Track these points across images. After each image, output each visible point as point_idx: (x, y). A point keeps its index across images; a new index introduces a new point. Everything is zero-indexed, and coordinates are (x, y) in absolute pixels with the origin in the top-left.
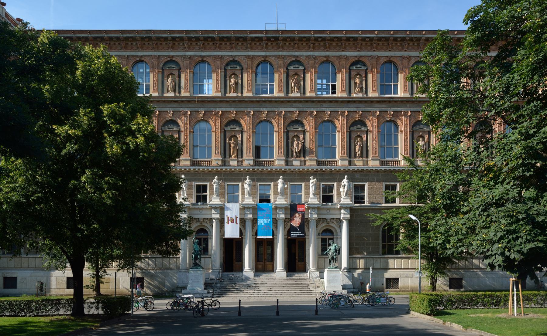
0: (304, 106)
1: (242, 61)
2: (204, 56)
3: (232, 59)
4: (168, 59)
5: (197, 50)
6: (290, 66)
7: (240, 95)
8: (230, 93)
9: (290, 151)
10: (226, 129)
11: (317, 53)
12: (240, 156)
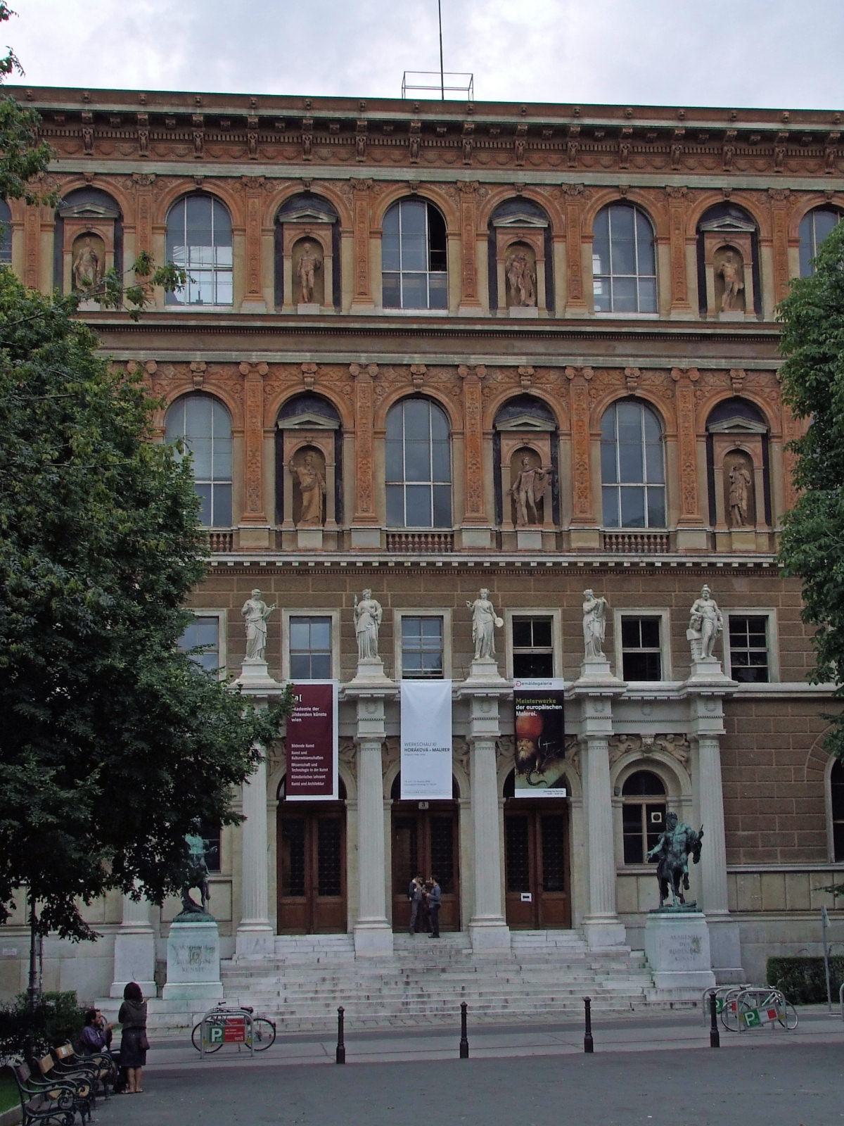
0: (551, 351)
1: (336, 193)
2: (206, 177)
3: (300, 189)
4: (78, 185)
5: (181, 158)
6: (499, 216)
7: (330, 311)
10: (285, 424)
11: (589, 178)
12: (331, 519)
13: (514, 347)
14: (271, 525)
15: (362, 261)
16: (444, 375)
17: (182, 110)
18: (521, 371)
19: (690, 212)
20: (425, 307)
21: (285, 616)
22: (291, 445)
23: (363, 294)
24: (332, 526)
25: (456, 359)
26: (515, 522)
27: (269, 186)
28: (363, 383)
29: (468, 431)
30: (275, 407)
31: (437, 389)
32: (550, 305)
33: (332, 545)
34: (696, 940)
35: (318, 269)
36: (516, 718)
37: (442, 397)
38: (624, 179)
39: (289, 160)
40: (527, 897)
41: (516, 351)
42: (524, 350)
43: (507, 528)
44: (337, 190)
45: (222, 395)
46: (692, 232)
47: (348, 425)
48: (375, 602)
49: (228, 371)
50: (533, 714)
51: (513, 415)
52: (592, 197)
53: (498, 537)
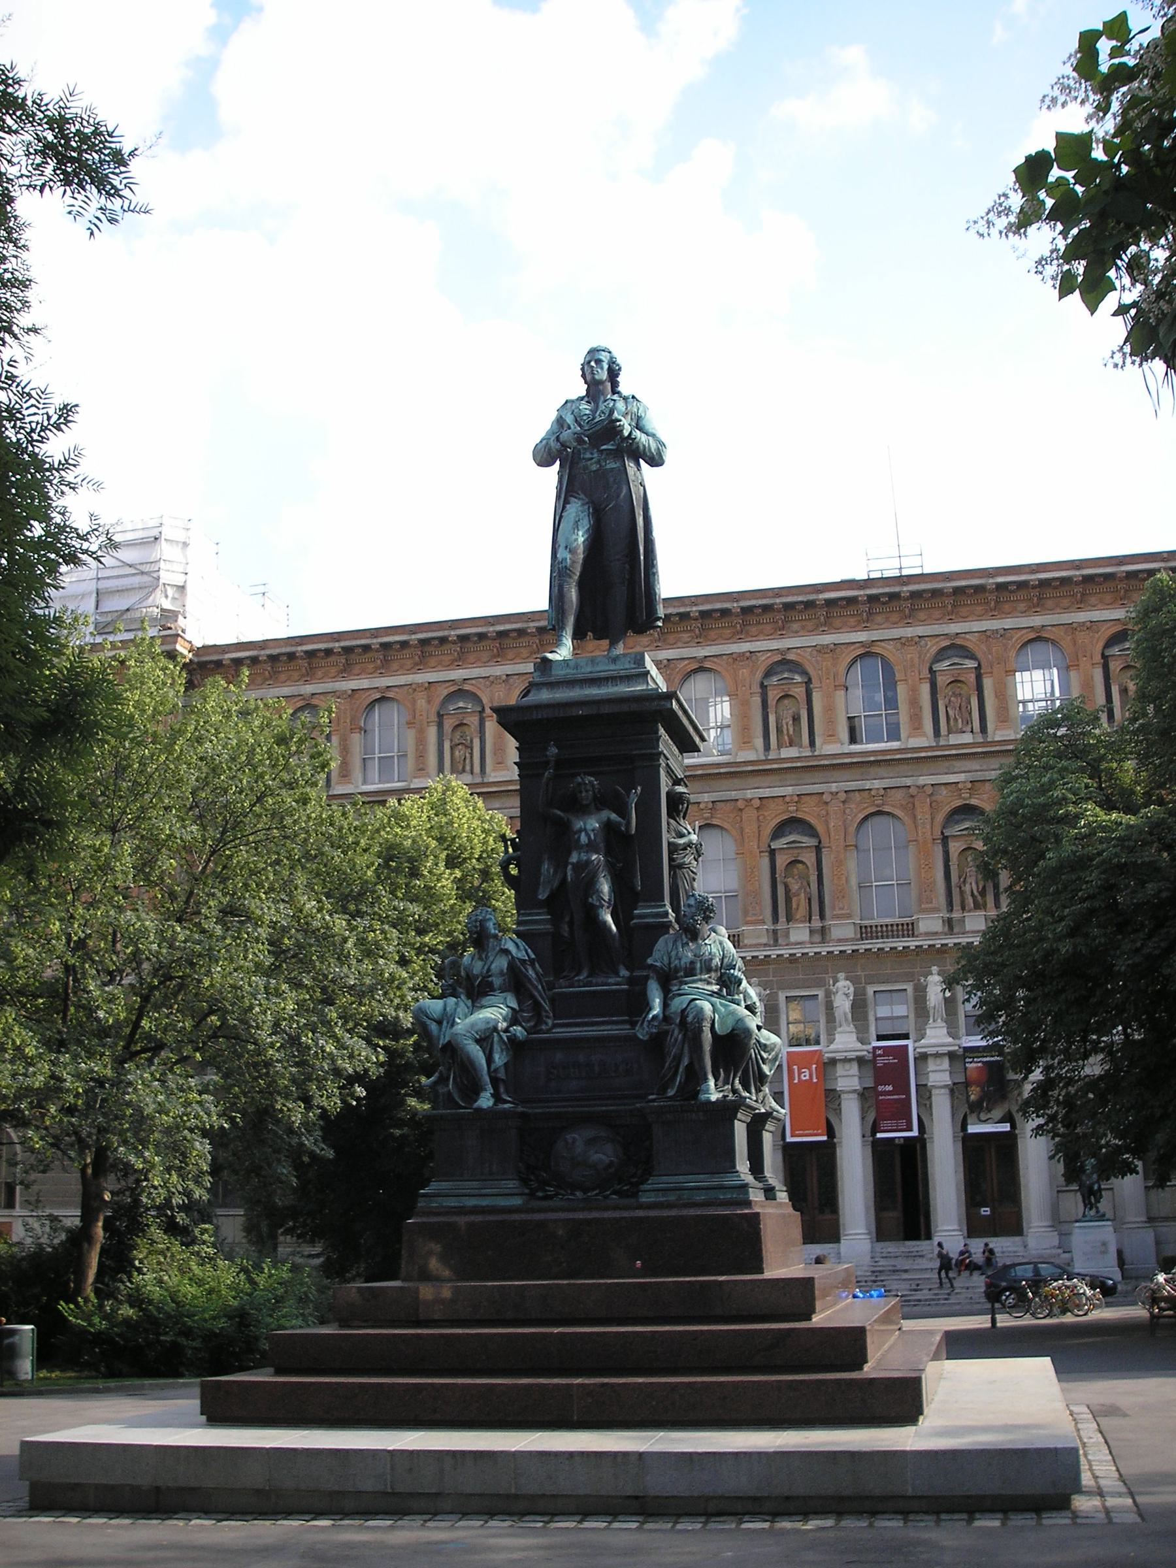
0: (985, 767)
3: (778, 658)
5: (686, 644)
6: (938, 661)
8: (779, 747)
9: (955, 892)
11: (1008, 623)
12: (816, 917)
13: (954, 767)
14: (769, 926)
15: (830, 709)
16: (899, 795)
17: (682, 610)
18: (960, 786)
19: (1095, 641)
20: (881, 740)
21: (782, 996)
22: (782, 861)
23: (831, 736)
24: (816, 923)
25: (908, 782)
26: (963, 909)
27: (754, 658)
28: (835, 807)
29: (920, 839)
30: (768, 831)
31: (893, 806)
32: (984, 729)
33: (817, 938)
34: (1104, 1244)
35: (796, 719)
36: (966, 1069)
37: (898, 812)
38: (1037, 621)
39: (770, 636)
40: (985, 1211)
41: (955, 770)
42: (963, 769)
43: (956, 915)
44: (807, 655)
45: (726, 825)
46: (1098, 658)
47: (825, 842)
48: (848, 982)
49: (729, 806)
50: (980, 1065)
51: (957, 822)
52: (1012, 638)
53: (949, 923)
